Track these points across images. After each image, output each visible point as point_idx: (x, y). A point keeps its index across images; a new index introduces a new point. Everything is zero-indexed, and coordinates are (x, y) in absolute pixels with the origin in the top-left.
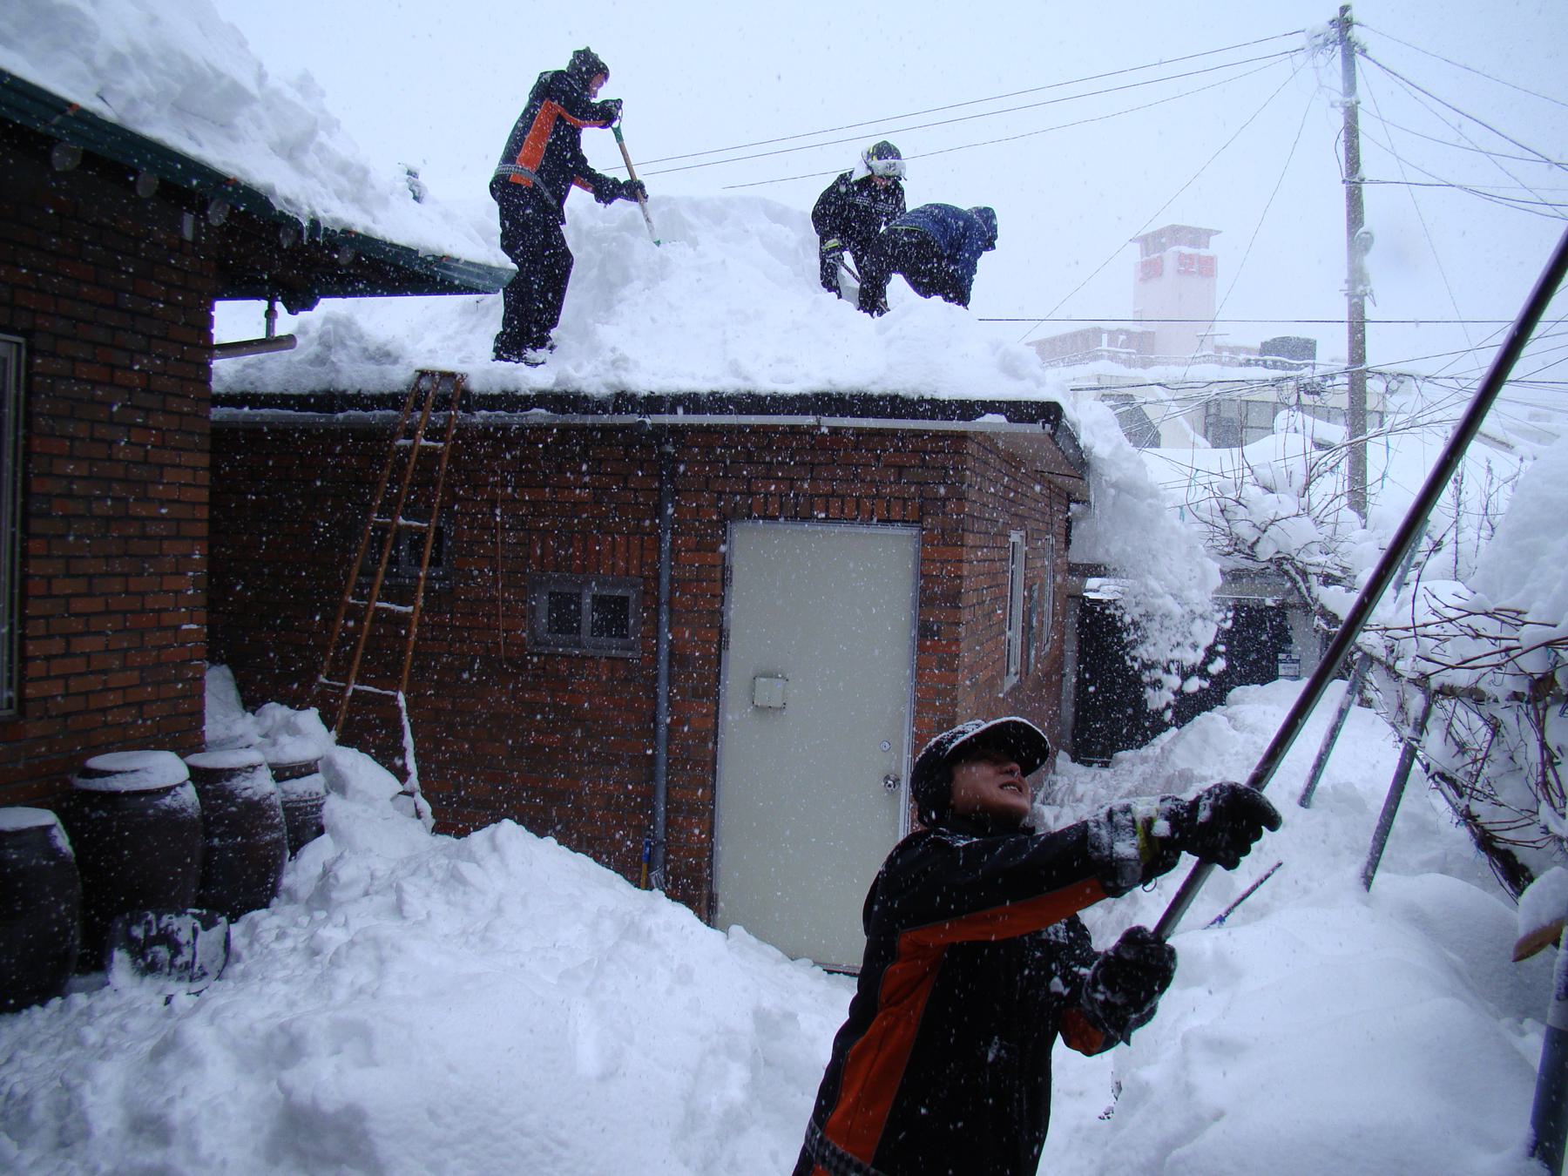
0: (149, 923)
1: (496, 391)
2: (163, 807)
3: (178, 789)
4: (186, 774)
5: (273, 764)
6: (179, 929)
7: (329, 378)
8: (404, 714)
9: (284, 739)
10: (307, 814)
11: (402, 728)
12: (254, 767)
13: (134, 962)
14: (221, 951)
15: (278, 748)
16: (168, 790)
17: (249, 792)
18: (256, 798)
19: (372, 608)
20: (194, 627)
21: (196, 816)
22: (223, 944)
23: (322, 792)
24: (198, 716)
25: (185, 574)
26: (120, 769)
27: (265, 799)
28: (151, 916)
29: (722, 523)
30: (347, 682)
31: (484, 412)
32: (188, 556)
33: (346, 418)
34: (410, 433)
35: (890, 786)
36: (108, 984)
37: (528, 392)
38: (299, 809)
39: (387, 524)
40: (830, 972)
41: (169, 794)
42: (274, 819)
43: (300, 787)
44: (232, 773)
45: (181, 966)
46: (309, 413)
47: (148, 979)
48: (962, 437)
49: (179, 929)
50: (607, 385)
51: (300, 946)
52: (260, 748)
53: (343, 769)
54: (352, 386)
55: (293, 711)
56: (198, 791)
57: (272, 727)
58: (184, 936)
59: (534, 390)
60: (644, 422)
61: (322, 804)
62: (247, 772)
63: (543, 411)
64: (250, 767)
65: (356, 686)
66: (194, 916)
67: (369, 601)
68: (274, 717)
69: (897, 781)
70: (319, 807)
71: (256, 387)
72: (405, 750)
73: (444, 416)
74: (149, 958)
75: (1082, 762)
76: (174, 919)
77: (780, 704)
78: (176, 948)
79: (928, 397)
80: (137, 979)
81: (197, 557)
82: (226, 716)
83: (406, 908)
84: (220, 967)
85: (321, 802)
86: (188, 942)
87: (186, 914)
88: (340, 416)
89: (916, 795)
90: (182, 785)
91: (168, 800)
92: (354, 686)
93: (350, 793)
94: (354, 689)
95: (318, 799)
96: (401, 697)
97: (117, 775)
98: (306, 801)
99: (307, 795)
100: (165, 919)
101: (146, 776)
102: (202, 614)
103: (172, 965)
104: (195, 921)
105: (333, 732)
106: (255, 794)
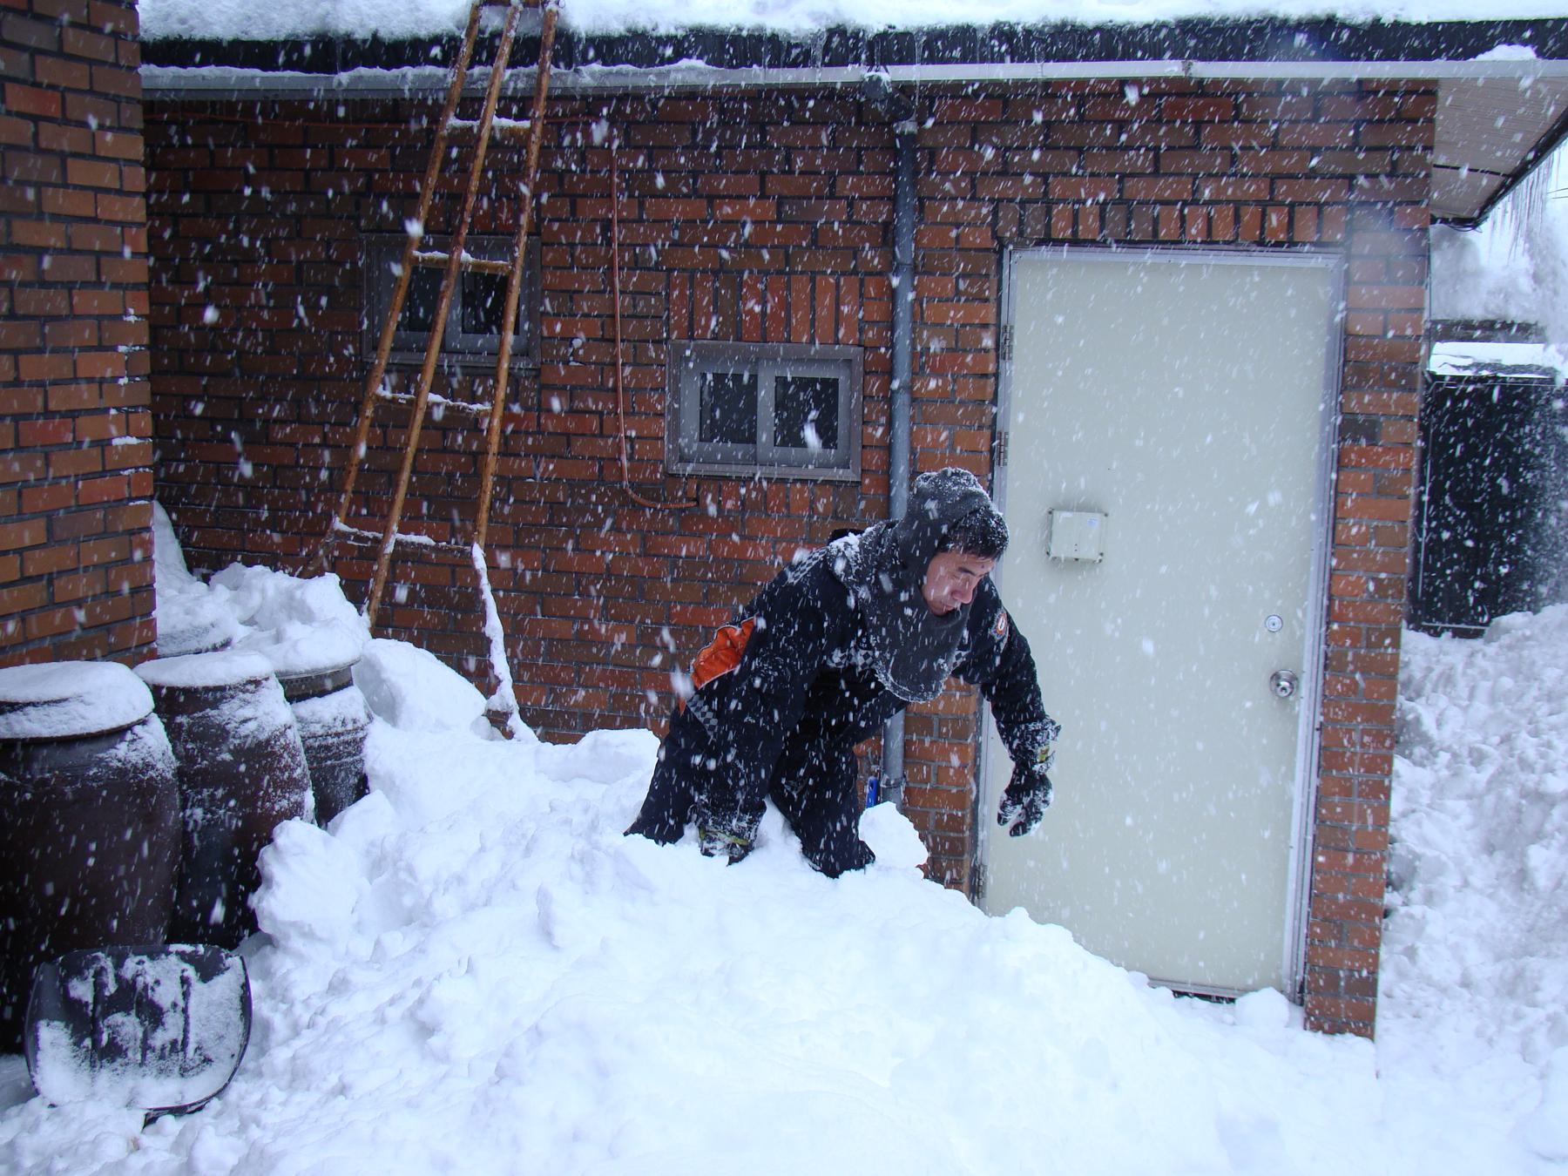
0: (99, 973)
1: (617, 28)
2: (115, 764)
3: (138, 729)
4: (146, 702)
5: (287, 673)
6: (157, 982)
7: (319, 11)
8: (485, 581)
9: (295, 630)
10: (338, 756)
11: (484, 603)
12: (257, 683)
13: (78, 1044)
14: (235, 1016)
15: (286, 645)
16: (118, 733)
17: (252, 726)
18: (263, 737)
19: (422, 405)
20: (133, 441)
21: (169, 776)
22: (237, 1003)
23: (363, 718)
24: (145, 593)
25: (115, 350)
26: (33, 698)
27: (277, 739)
28: (108, 963)
29: (998, 251)
30: (386, 530)
31: (597, 67)
32: (118, 318)
33: (354, 80)
34: (470, 105)
35: (1284, 689)
36: (37, 1093)
37: (672, 32)
38: (328, 748)
39: (439, 261)
40: (1178, 994)
41: (123, 740)
42: (293, 770)
43: (327, 710)
44: (217, 694)
45: (163, 1048)
46: (288, 74)
47: (105, 1076)
48: (1427, 91)
49: (157, 982)
50: (815, 17)
51: (393, 1013)
52: (250, 645)
53: (393, 679)
54: (362, 26)
55: (296, 581)
56: (168, 727)
57: (261, 607)
58: (166, 995)
59: (683, 27)
60: (879, 79)
61: (364, 738)
62: (248, 691)
63: (700, 64)
64: (250, 682)
65: (401, 537)
66: (182, 956)
67: (417, 394)
68: (263, 591)
69: (1293, 680)
70: (358, 744)
71: (192, 28)
72: (489, 641)
73: (528, 76)
74: (105, 1038)
75: (1427, 630)
76: (148, 964)
77: (1092, 554)
78: (153, 1015)
79: (1387, 19)
80: (85, 1076)
81: (132, 319)
82: (181, 591)
83: (558, 931)
84: (236, 1049)
85: (361, 735)
86: (175, 1005)
87: (168, 953)
88: (344, 77)
89: (1328, 700)
90: (143, 722)
91: (122, 750)
92: (396, 536)
93: (403, 718)
94: (398, 543)
95: (356, 730)
96: (478, 553)
97: (30, 709)
98: (338, 735)
99: (339, 723)
100: (131, 966)
101: (81, 708)
102: (145, 421)
103: (146, 1047)
104: (186, 966)
105: (366, 616)
106: (261, 728)
